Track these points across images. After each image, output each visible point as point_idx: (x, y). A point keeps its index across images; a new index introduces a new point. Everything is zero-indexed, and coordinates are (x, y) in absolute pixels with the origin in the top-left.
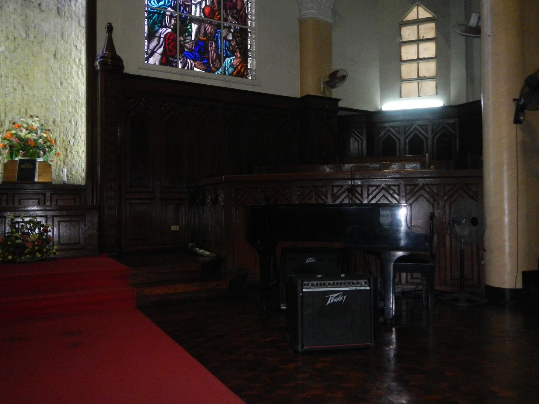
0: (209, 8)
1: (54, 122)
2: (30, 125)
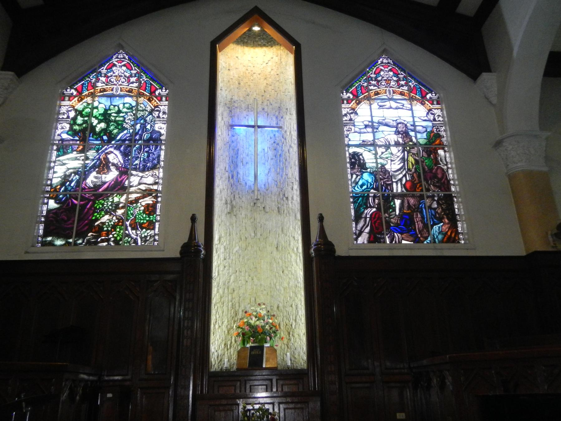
0: (410, 182)
1: (278, 307)
2: (259, 313)
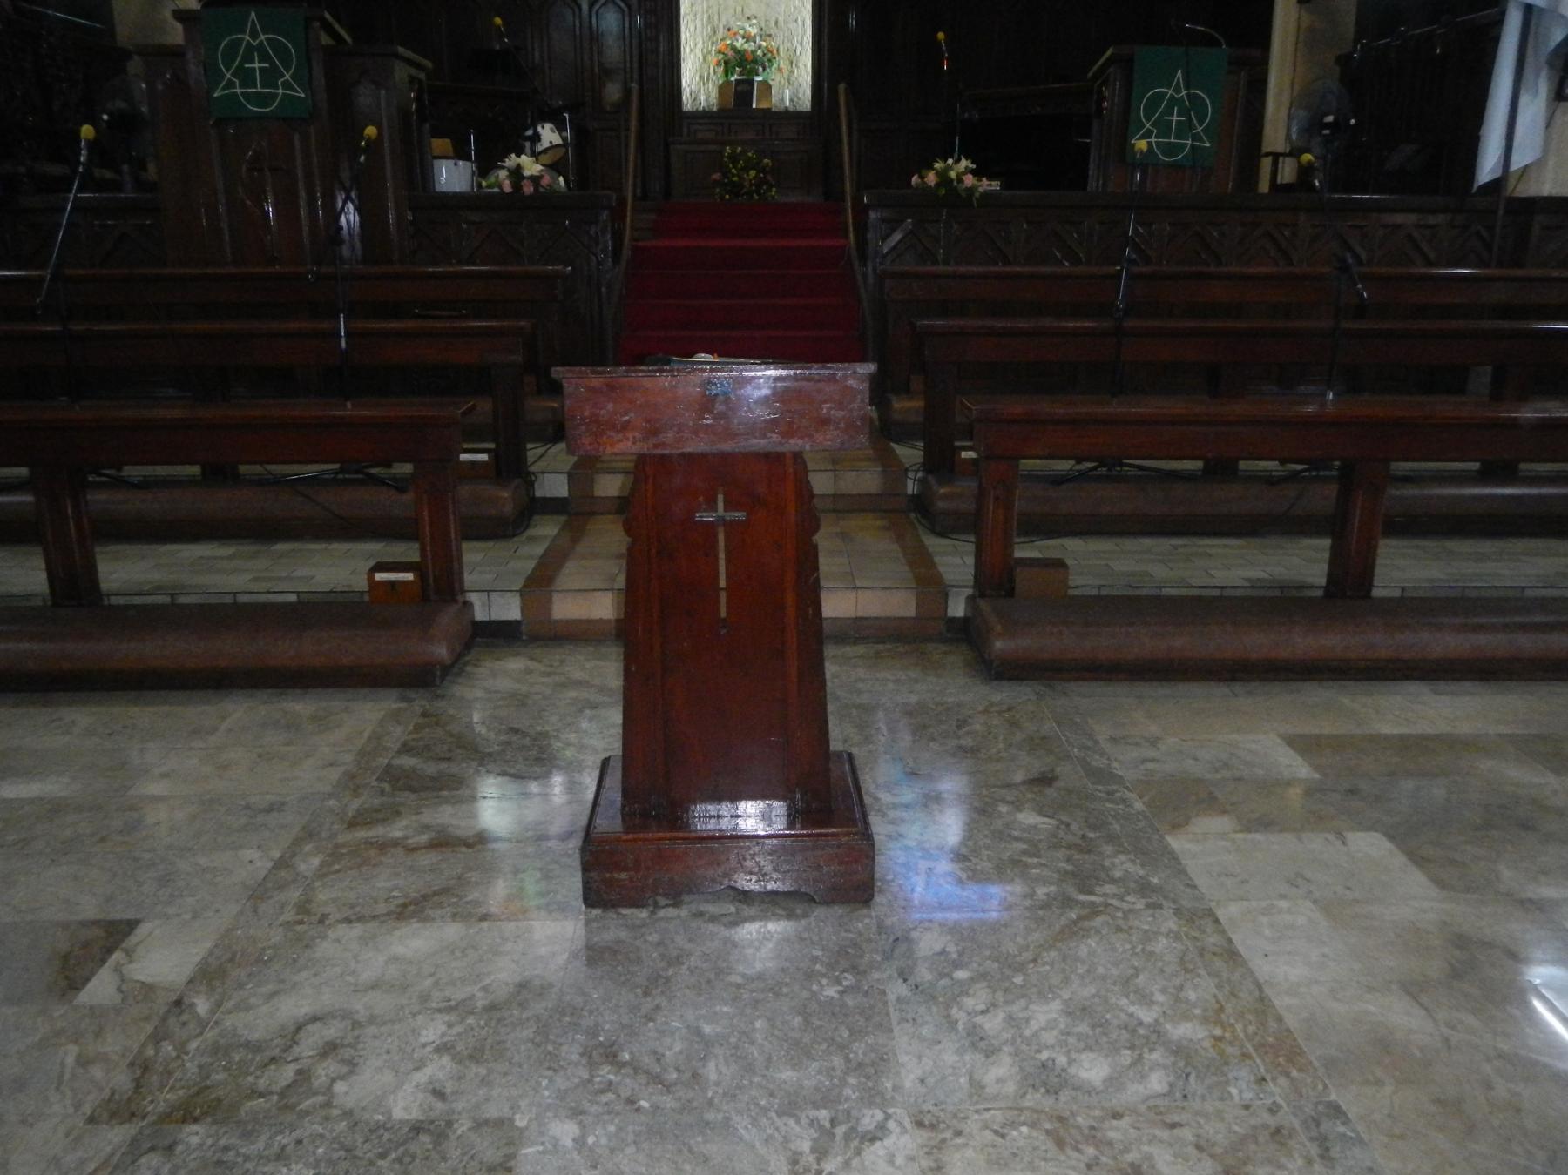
1: (776, 23)
